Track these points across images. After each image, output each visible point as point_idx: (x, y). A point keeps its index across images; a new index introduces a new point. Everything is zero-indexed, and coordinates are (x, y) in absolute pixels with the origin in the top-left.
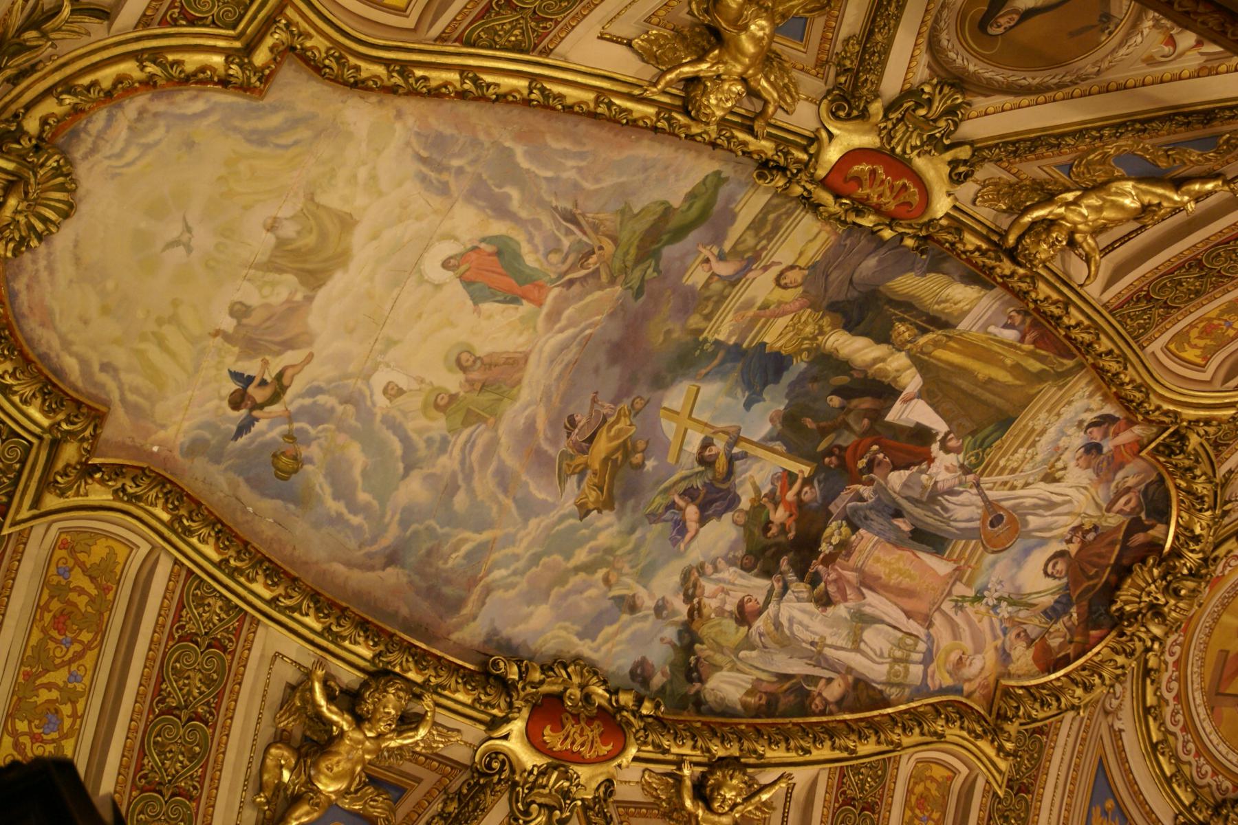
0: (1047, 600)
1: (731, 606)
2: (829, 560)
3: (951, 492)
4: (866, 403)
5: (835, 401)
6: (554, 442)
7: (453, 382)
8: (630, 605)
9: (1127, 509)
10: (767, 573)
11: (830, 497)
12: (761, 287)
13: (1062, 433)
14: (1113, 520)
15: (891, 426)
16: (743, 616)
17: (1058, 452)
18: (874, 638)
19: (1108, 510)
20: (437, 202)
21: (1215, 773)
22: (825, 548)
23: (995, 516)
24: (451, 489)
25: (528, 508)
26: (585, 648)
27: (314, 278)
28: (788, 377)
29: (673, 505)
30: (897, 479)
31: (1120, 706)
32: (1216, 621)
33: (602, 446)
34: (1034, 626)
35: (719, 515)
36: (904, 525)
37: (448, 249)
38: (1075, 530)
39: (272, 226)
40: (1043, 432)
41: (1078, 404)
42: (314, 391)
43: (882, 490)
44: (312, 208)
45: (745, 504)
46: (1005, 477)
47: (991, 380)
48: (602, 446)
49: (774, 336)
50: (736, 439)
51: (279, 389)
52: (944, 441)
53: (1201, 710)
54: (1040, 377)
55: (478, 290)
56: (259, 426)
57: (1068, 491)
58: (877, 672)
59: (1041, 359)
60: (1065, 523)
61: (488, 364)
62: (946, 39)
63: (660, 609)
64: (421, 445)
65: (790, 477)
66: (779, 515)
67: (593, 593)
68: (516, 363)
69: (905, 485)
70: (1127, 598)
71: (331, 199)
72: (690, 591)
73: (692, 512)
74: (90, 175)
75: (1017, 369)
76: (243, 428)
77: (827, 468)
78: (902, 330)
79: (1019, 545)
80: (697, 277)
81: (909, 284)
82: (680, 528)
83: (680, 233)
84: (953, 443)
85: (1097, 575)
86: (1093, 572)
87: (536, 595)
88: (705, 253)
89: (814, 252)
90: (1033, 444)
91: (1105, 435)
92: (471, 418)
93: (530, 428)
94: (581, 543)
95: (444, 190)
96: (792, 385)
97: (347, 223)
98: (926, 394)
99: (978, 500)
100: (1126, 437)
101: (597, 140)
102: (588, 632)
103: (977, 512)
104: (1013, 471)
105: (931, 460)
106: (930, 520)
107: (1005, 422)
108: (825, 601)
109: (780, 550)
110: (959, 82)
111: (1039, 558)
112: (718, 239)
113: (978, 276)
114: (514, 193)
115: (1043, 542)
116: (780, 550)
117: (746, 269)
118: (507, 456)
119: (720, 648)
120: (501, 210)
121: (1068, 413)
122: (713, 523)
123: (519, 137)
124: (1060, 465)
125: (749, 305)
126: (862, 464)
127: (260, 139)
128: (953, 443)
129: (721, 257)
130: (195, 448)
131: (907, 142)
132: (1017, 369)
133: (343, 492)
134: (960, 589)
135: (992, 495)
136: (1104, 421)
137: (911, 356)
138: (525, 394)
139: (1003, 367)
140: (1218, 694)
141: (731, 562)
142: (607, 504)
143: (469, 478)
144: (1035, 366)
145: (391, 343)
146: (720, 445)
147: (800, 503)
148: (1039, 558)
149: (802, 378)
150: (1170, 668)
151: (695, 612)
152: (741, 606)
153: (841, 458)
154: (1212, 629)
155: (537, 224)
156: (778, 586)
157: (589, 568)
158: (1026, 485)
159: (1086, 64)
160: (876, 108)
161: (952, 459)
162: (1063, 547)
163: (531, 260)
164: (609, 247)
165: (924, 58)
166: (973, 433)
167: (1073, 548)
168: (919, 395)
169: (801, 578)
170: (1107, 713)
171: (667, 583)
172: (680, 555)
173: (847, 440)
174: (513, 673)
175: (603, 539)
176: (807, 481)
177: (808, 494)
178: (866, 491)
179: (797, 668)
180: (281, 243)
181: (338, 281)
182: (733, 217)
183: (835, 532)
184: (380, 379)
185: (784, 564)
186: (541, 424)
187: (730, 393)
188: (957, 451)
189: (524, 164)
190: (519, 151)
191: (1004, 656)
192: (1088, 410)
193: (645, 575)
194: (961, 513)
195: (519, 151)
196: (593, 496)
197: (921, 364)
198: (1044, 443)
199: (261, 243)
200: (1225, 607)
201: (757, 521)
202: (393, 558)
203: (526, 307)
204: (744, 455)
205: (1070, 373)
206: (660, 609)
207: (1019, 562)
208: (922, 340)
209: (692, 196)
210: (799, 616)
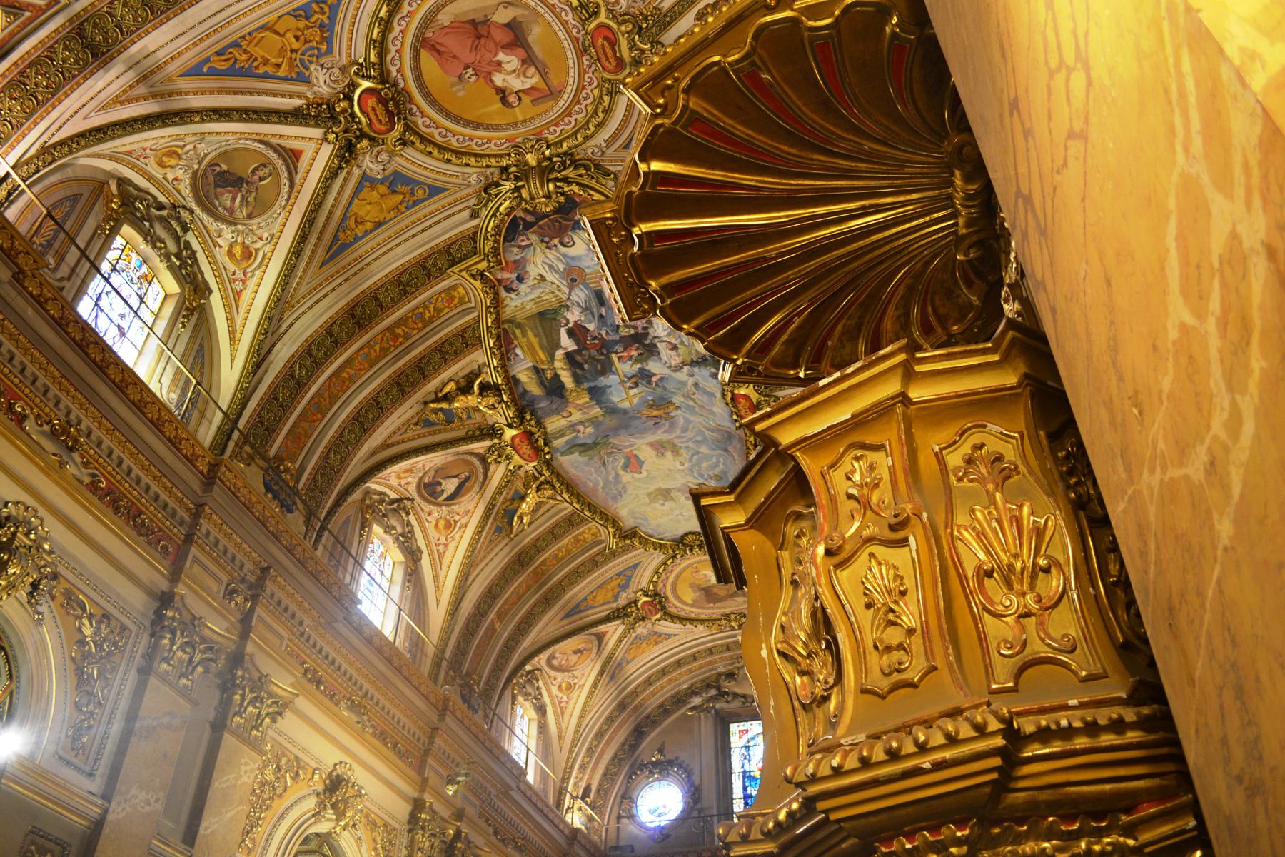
1: (673, 353)
3: (579, 305)
4: (578, 358)
5: (586, 366)
6: (664, 425)
7: (669, 454)
8: (696, 385)
9: (525, 238)
10: (655, 346)
11: (615, 342)
12: (576, 416)
13: (526, 295)
14: (534, 238)
15: (577, 344)
16: (675, 348)
17: (533, 288)
19: (532, 244)
20: (628, 486)
21: (585, 72)
22: (632, 331)
23: (572, 282)
24: (698, 442)
25: (688, 422)
26: (719, 395)
27: (668, 491)
28: (592, 384)
30: (591, 327)
31: (596, 146)
32: (525, 121)
33: (655, 413)
35: (649, 371)
36: (603, 311)
37: (636, 475)
38: (549, 248)
40: (533, 300)
41: (513, 304)
43: (598, 328)
45: (639, 365)
46: (558, 293)
47: (535, 336)
48: (655, 413)
50: (623, 382)
52: (566, 325)
53: (565, 97)
54: (519, 326)
55: (641, 464)
57: (540, 266)
59: (514, 334)
60: (551, 254)
61: (657, 450)
62: (481, 480)
63: (692, 376)
64: (690, 453)
65: (619, 358)
68: (651, 445)
69: (590, 322)
72: (679, 368)
73: (654, 379)
75: (524, 335)
77: (607, 350)
79: (574, 264)
80: (590, 430)
81: (535, 390)
82: (662, 379)
83: (583, 445)
84: (564, 321)
85: (557, 221)
86: (557, 224)
87: (714, 413)
88: (582, 436)
89: (554, 418)
90: (539, 297)
91: (512, 282)
92: (674, 445)
93: (666, 432)
94: (688, 405)
95: (624, 487)
96: (593, 381)
97: (649, 494)
98: (558, 346)
99: (573, 293)
100: (506, 275)
102: (712, 395)
103: (577, 290)
104: (553, 293)
105: (575, 322)
106: (594, 303)
107: (542, 315)
109: (645, 346)
111: (571, 252)
112: (576, 437)
113: (513, 382)
114: (610, 478)
115: (564, 255)
116: (645, 346)
117: (575, 424)
118: (678, 432)
119: (690, 352)
120: (617, 475)
121: (518, 302)
122: (654, 371)
123: (595, 490)
124: (536, 281)
125: (584, 413)
126: (596, 341)
127: (646, 519)
128: (564, 321)
129: (579, 431)
132: (524, 335)
133: (717, 465)
135: (566, 290)
136: (509, 289)
137: (553, 363)
138: (657, 438)
139: (528, 339)
140: (552, 93)
141: (661, 359)
142: (671, 402)
143: (691, 439)
144: (518, 332)
145: (670, 470)
146: (628, 384)
147: (625, 349)
148: (571, 252)
149: (589, 381)
150: (561, 127)
151: (684, 364)
152: (672, 349)
153: (601, 349)
154: (530, 119)
155: (613, 468)
156: (657, 340)
157: (694, 400)
158: (553, 283)
161: (569, 316)
162: (559, 246)
163: (623, 461)
164: (602, 452)
166: (555, 319)
167: (556, 241)
168: (561, 347)
169: (648, 334)
170: (603, 152)
171: (682, 375)
172: (670, 376)
173: (594, 352)
175: (682, 399)
176: (616, 352)
178: (603, 333)
180: (666, 500)
181: (664, 487)
182: (567, 442)
184: (681, 468)
185: (648, 342)
186: (662, 430)
187: (611, 393)
188: (565, 317)
189: (602, 484)
190: (600, 487)
192: (511, 299)
193: (684, 383)
194: (582, 295)
195: (600, 487)
196: (671, 407)
197: (552, 357)
199: (669, 505)
200: (516, 124)
202: (726, 450)
203: (635, 452)
204: (625, 376)
205: (509, 321)
207: (579, 258)
208: (545, 367)
209: (572, 453)
210: (661, 329)
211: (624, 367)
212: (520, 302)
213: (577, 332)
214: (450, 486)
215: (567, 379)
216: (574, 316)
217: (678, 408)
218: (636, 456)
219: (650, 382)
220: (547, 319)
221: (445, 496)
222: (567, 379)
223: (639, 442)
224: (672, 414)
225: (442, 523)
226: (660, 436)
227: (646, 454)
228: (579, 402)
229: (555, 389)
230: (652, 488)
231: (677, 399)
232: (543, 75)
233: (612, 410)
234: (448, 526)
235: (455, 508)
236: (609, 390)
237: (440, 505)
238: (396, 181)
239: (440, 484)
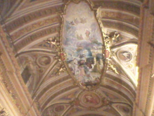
0: (86, 82)
2: (81, 67)
4: (91, 62)
7: (79, 35)
8: (71, 56)
11: (85, 64)
12: (96, 51)
16: (75, 63)
17: (95, 76)
18: (78, 73)
25: (74, 46)
27: (81, 22)
29: (79, 54)
30: (88, 68)
34: (84, 82)
36: (85, 70)
37: (88, 30)
39: (83, 17)
42: (74, 27)
43: (87, 67)
44: (85, 19)
49: (93, 54)
50: (85, 56)
51: (73, 24)
55: (86, 34)
56: (70, 25)
58: (76, 74)
62: (119, 51)
65: (84, 61)
66: (82, 62)
67: (71, 53)
70: (88, 87)
71: (87, 20)
72: (75, 59)
73: (79, 56)
74: (80, 4)
76: (70, 24)
78: (98, 62)
80: (94, 47)
81: (101, 60)
82: (78, 56)
89: (100, 53)
97: (86, 22)
101: (100, 34)
108: (78, 68)
110: (116, 54)
127: (88, 13)
130: (67, 22)
131: (110, 54)
134: (83, 76)
136: (98, 78)
159: (121, 60)
160: (112, 50)
165: (117, 51)
171: (74, 57)
174: (64, 51)
177: (84, 63)
179: (73, 69)
182: (99, 46)
183: (83, 66)
191: (81, 81)
193: (74, 56)
197: (96, 64)
198: (95, 75)
201: (81, 60)
202: (67, 39)
206: (72, 58)
209: (99, 43)
211: (84, 59)
212: (98, 75)
213: (91, 67)
214: (125, 54)
215: (95, 59)
216: (90, 70)
217: (76, 49)
218: (87, 36)
219: (80, 55)
220: (95, 71)
221: (127, 53)
222: (95, 59)
223: (86, 40)
224: (77, 47)
225: (131, 49)
226: (81, 41)
227: (84, 36)
228: (94, 54)
229: (98, 59)
230: (85, 24)
231: (75, 51)
232: (86, 98)
233: (89, 50)
234: (130, 49)
235: (127, 50)
236: (88, 55)
237: (130, 52)
238: (107, 96)
239: (127, 56)
